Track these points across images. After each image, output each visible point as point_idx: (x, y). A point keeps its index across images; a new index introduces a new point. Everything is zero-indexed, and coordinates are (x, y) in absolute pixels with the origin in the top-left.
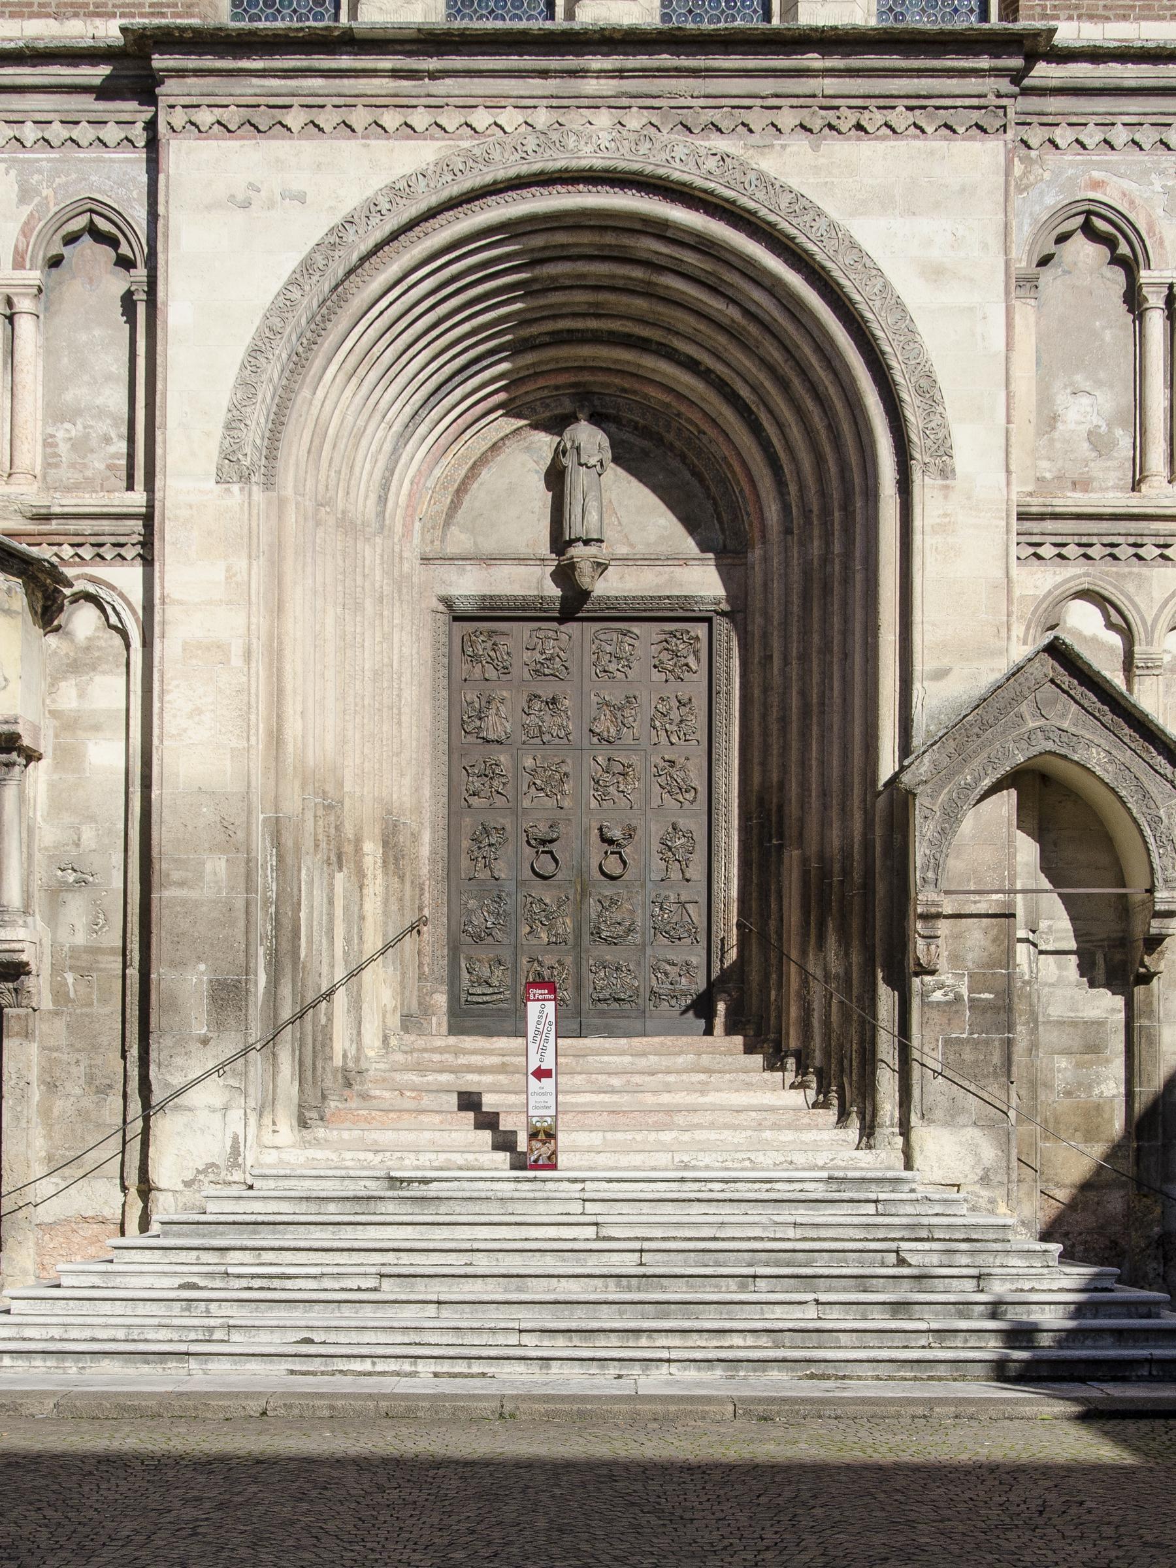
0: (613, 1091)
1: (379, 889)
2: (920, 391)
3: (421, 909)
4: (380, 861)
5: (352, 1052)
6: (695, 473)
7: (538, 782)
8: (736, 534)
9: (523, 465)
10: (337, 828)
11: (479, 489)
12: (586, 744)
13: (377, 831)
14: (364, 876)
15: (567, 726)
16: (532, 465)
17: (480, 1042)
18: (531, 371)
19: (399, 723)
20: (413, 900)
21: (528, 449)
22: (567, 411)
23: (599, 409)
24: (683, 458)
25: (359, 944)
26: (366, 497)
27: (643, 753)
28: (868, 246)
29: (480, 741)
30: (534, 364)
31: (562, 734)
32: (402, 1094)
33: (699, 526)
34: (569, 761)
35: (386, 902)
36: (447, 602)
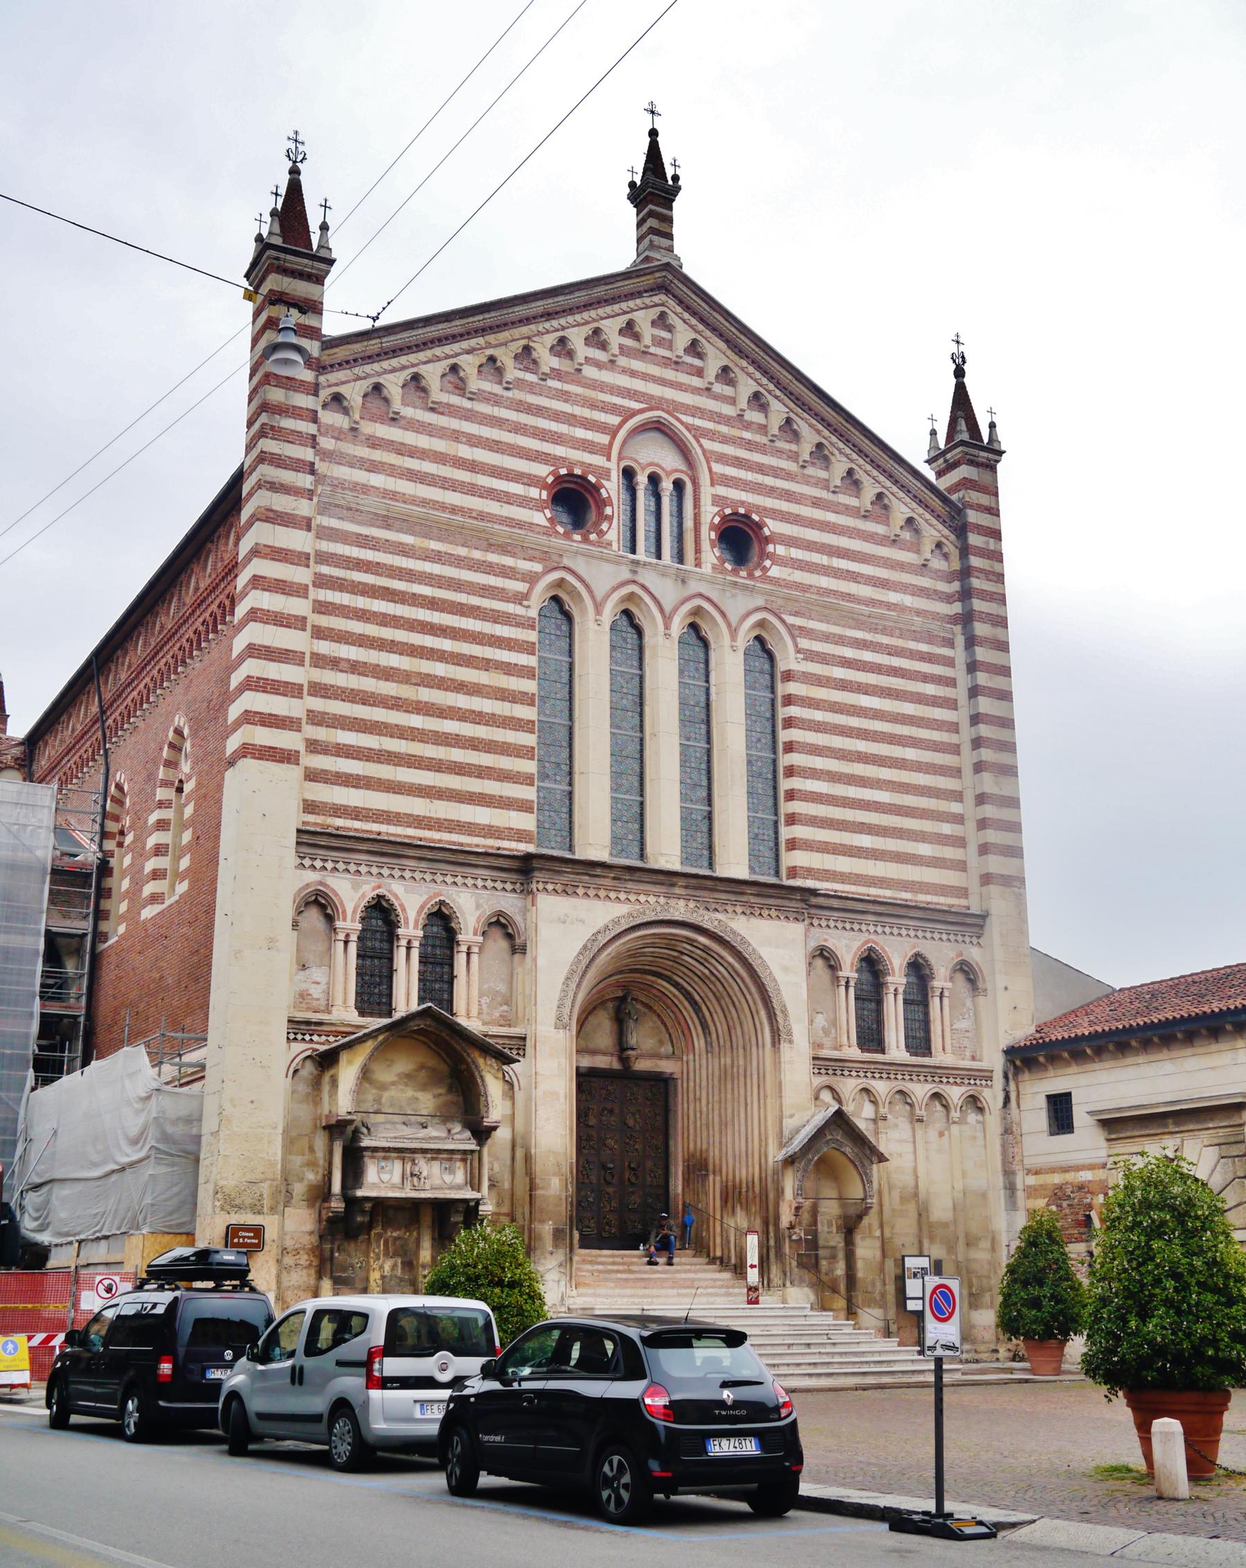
21: (605, 1009)
24: (659, 1016)
28: (765, 958)
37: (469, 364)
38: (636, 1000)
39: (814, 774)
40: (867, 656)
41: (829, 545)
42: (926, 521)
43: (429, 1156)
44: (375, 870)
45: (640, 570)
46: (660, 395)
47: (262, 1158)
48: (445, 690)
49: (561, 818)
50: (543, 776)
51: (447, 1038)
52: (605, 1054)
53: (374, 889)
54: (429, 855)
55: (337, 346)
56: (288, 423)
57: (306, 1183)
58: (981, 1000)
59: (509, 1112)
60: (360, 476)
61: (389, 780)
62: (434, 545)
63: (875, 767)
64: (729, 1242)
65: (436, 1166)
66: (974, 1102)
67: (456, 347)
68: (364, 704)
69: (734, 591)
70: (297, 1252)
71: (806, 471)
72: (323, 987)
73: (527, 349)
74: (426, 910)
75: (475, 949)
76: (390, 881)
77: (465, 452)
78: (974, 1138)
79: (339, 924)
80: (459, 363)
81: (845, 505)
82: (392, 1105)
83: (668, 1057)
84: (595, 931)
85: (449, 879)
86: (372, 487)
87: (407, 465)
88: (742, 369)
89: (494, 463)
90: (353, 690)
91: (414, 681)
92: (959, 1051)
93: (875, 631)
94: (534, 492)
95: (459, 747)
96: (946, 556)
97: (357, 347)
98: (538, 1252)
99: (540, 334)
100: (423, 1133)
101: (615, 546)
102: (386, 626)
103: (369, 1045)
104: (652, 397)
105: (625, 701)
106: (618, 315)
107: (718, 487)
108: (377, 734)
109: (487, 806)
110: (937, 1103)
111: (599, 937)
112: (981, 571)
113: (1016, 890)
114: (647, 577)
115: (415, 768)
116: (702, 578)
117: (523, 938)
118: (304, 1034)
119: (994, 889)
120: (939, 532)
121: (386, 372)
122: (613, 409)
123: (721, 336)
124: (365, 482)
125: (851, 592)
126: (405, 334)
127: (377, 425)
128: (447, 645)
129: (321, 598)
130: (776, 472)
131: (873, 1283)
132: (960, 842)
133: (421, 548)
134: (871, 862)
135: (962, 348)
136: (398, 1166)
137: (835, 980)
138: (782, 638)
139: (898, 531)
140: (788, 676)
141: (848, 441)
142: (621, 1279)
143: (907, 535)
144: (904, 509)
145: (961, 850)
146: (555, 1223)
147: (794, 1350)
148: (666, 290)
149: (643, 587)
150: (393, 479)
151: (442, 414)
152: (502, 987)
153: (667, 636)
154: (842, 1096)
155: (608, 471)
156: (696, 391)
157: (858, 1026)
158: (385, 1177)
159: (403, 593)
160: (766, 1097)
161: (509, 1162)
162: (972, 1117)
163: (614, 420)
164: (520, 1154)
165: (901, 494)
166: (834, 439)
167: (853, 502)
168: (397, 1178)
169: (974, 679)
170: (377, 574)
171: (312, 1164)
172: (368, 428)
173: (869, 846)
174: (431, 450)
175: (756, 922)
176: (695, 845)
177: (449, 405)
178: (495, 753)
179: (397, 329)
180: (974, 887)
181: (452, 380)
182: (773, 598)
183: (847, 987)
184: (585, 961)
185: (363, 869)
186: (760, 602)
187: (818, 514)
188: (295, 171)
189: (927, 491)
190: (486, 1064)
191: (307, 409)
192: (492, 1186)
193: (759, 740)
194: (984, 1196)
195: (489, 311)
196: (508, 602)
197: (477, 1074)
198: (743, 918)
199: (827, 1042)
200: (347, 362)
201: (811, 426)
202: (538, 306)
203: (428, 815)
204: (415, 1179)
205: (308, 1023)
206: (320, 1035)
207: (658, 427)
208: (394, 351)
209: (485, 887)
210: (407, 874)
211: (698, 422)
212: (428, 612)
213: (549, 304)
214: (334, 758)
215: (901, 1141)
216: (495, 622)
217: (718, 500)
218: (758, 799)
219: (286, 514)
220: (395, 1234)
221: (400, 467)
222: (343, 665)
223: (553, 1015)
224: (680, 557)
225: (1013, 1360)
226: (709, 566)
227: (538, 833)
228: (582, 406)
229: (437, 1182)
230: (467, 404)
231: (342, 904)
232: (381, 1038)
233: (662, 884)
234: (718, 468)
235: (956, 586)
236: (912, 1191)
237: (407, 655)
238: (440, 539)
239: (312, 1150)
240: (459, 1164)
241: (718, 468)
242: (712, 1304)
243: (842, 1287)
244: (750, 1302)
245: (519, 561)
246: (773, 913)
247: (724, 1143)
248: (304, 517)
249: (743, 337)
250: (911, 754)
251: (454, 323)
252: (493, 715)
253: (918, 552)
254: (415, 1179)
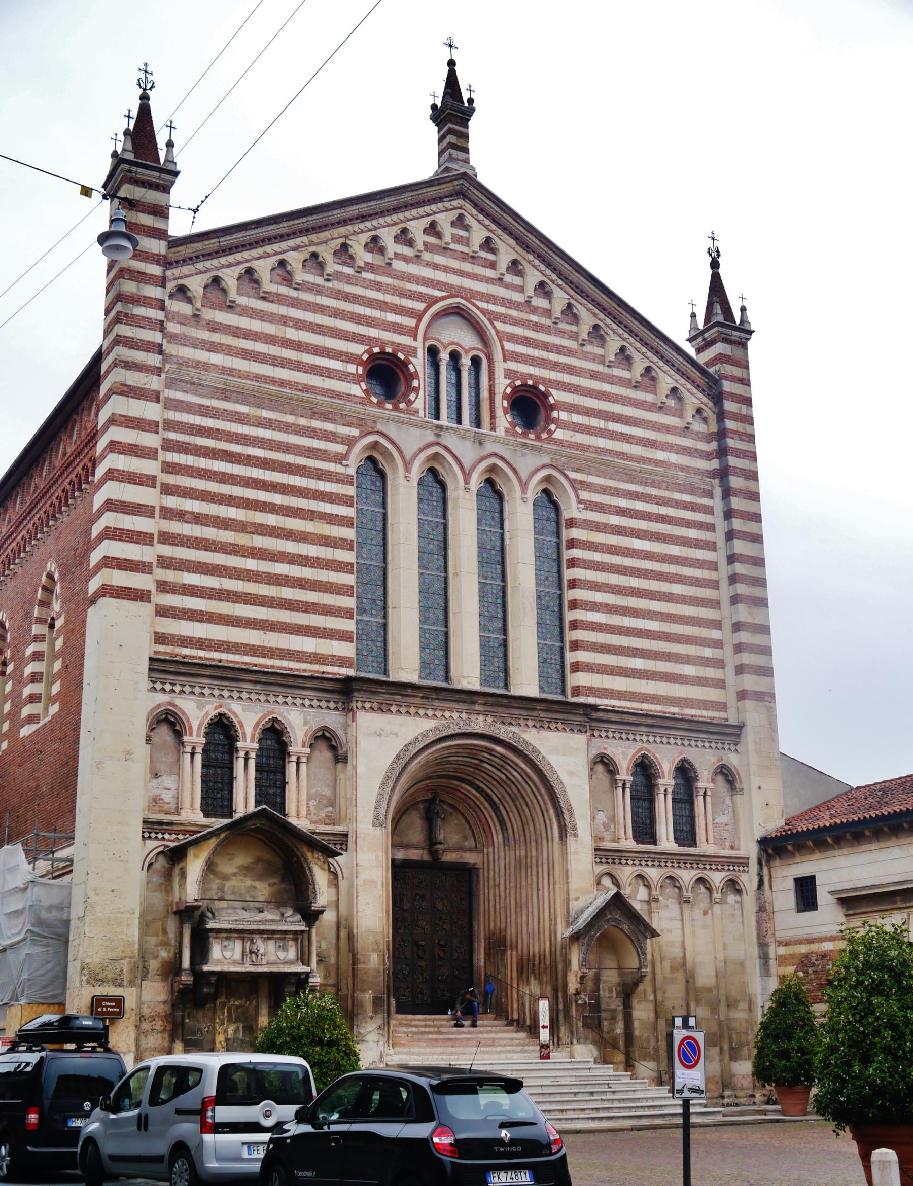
2: (568, 810)
21: (417, 810)
24: (463, 815)
37: (295, 259)
38: (443, 801)
39: (594, 607)
40: (639, 506)
41: (605, 411)
42: (688, 390)
43: (265, 936)
44: (216, 692)
45: (443, 433)
46: (459, 284)
47: (122, 939)
48: (277, 537)
49: (377, 647)
50: (361, 610)
51: (280, 835)
52: (416, 848)
53: (216, 708)
54: (264, 679)
55: (181, 245)
56: (140, 311)
57: (160, 959)
58: (738, 798)
59: (334, 898)
60: (202, 355)
61: (228, 615)
62: (266, 414)
63: (647, 601)
64: (524, 1007)
65: (271, 945)
66: (733, 885)
67: (283, 245)
68: (206, 550)
69: (524, 451)
70: (152, 1019)
71: (585, 349)
72: (173, 792)
73: (345, 247)
74: (261, 726)
75: (304, 759)
76: (229, 701)
77: (292, 334)
78: (733, 915)
79: (186, 738)
80: (286, 258)
81: (618, 377)
82: (233, 893)
83: (470, 850)
84: (407, 743)
85: (280, 699)
86: (213, 364)
87: (242, 346)
88: (529, 262)
89: (317, 343)
90: (196, 538)
91: (249, 530)
92: (720, 842)
93: (645, 484)
94: (351, 368)
95: (288, 586)
96: (705, 420)
97: (198, 246)
98: (360, 1017)
99: (355, 233)
100: (260, 917)
101: (421, 413)
102: (224, 483)
103: (213, 842)
104: (452, 286)
105: (431, 546)
106: (423, 217)
107: (509, 362)
108: (218, 576)
109: (313, 637)
110: (701, 886)
111: (410, 748)
112: (735, 432)
113: (767, 704)
114: (450, 440)
115: (251, 604)
116: (497, 440)
117: (344, 749)
118: (157, 833)
119: (749, 704)
120: (699, 399)
121: (223, 267)
122: (419, 297)
123: (511, 234)
124: (206, 360)
125: (625, 451)
126: (240, 235)
127: (217, 312)
128: (277, 499)
129: (169, 459)
130: (559, 350)
131: (648, 1040)
132: (719, 664)
133: (255, 416)
134: (644, 682)
135: (716, 244)
136: (238, 945)
137: (614, 782)
138: (565, 491)
139: (664, 399)
140: (571, 523)
141: (620, 322)
142: (432, 1039)
143: (671, 403)
144: (669, 380)
145: (721, 671)
146: (374, 993)
147: (580, 1097)
148: (464, 195)
149: (446, 448)
150: (230, 358)
151: (272, 302)
152: (327, 792)
153: (467, 489)
154: (620, 881)
155: (415, 349)
156: (489, 281)
157: (633, 822)
158: (228, 954)
159: (240, 455)
160: (554, 883)
161: (334, 941)
162: (732, 898)
163: (421, 306)
164: (343, 933)
165: (666, 368)
166: (608, 321)
167: (625, 374)
168: (237, 955)
169: (730, 524)
170: (217, 439)
171: (165, 944)
172: (209, 314)
173: (642, 667)
174: (262, 333)
175: (545, 734)
176: (492, 668)
177: (277, 294)
178: (320, 591)
179: (233, 230)
180: (732, 700)
181: (280, 273)
182: (557, 457)
183: (624, 788)
184: (398, 769)
185: (207, 691)
186: (546, 460)
187: (596, 385)
188: (144, 98)
189: (688, 365)
190: (313, 857)
191: (156, 299)
192: (319, 962)
193: (547, 578)
194: (742, 964)
195: (311, 214)
196: (329, 461)
197: (305, 865)
198: (534, 731)
199: (607, 835)
200: (191, 259)
201: (589, 310)
202: (354, 210)
203: (262, 644)
204: (253, 956)
205: (160, 823)
206: (170, 834)
207: (457, 312)
208: (230, 249)
209: (311, 706)
210: (245, 695)
211: (492, 307)
212: (261, 471)
213: (363, 207)
214: (180, 597)
215: (671, 919)
216: (319, 479)
217: (509, 374)
218: (546, 628)
219: (138, 388)
220: (237, 1003)
221: (236, 348)
222: (187, 516)
223: (370, 815)
224: (477, 422)
225: (768, 1103)
226: (503, 429)
227: (357, 659)
228: (392, 294)
229: (273, 958)
230: (293, 293)
231: (188, 721)
232: (222, 836)
233: (464, 702)
234: (509, 346)
235: (714, 445)
236: (681, 961)
237: (243, 508)
238: (270, 409)
239: (165, 931)
240: (291, 943)
241: (509, 346)
242: (510, 1059)
243: (621, 1044)
244: (542, 1057)
245: (339, 427)
246: (560, 726)
247: (519, 923)
248: (154, 391)
249: (529, 235)
250: (677, 589)
251: (281, 225)
252: (318, 558)
253: (681, 416)
254: (253, 956)
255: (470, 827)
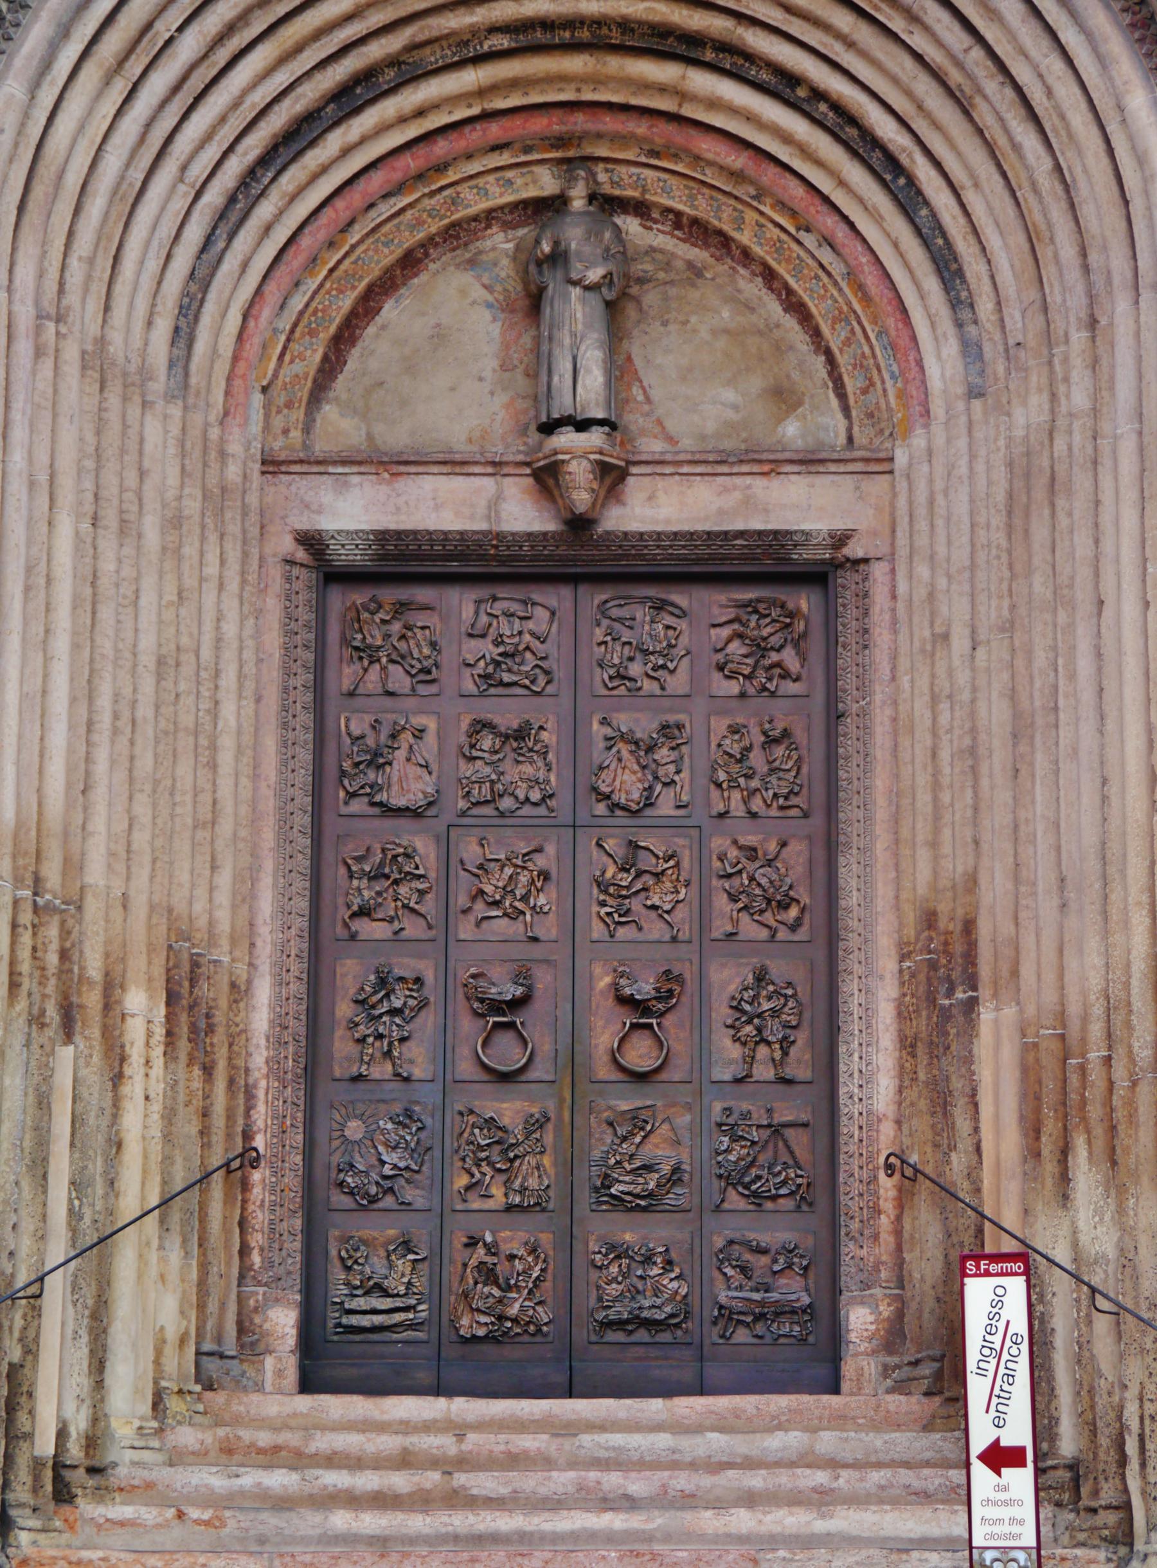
0: (630, 1503)
1: (157, 1088)
3: (247, 1136)
4: (159, 1031)
5: (79, 1424)
6: (796, 307)
7: (488, 889)
8: (871, 415)
9: (463, 292)
10: (64, 955)
11: (377, 336)
12: (583, 817)
13: (159, 971)
14: (123, 1059)
15: (548, 782)
16: (479, 293)
17: (357, 1406)
18: (475, 111)
19: (213, 766)
20: (230, 1117)
21: (472, 263)
22: (546, 193)
23: (607, 189)
24: (769, 276)
25: (106, 1196)
26: (149, 323)
27: (694, 833)
29: (376, 811)
30: (482, 92)
31: (535, 796)
32: (180, 1515)
33: (800, 403)
34: (551, 849)
35: (169, 1116)
36: (312, 542)
38: (640, 209)
142: (350, 1539)
255: (816, 334)
